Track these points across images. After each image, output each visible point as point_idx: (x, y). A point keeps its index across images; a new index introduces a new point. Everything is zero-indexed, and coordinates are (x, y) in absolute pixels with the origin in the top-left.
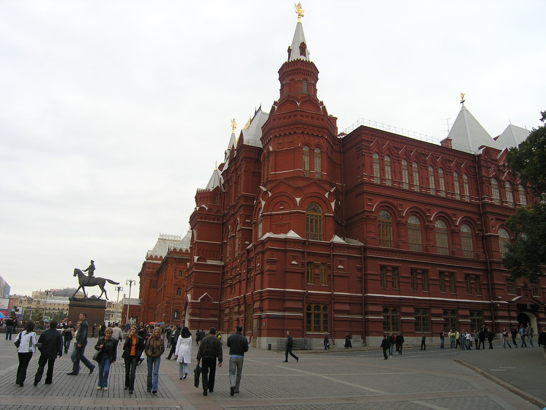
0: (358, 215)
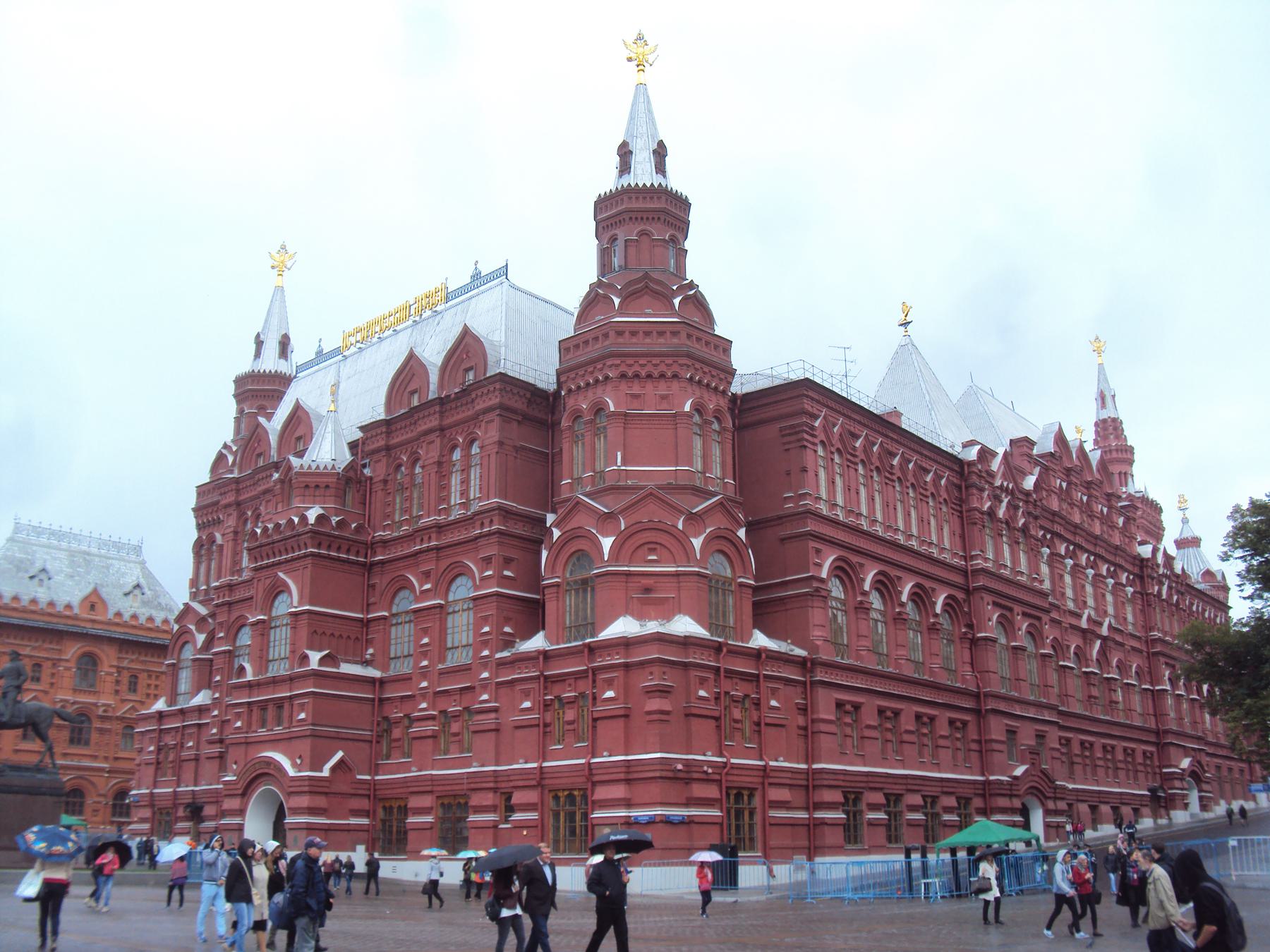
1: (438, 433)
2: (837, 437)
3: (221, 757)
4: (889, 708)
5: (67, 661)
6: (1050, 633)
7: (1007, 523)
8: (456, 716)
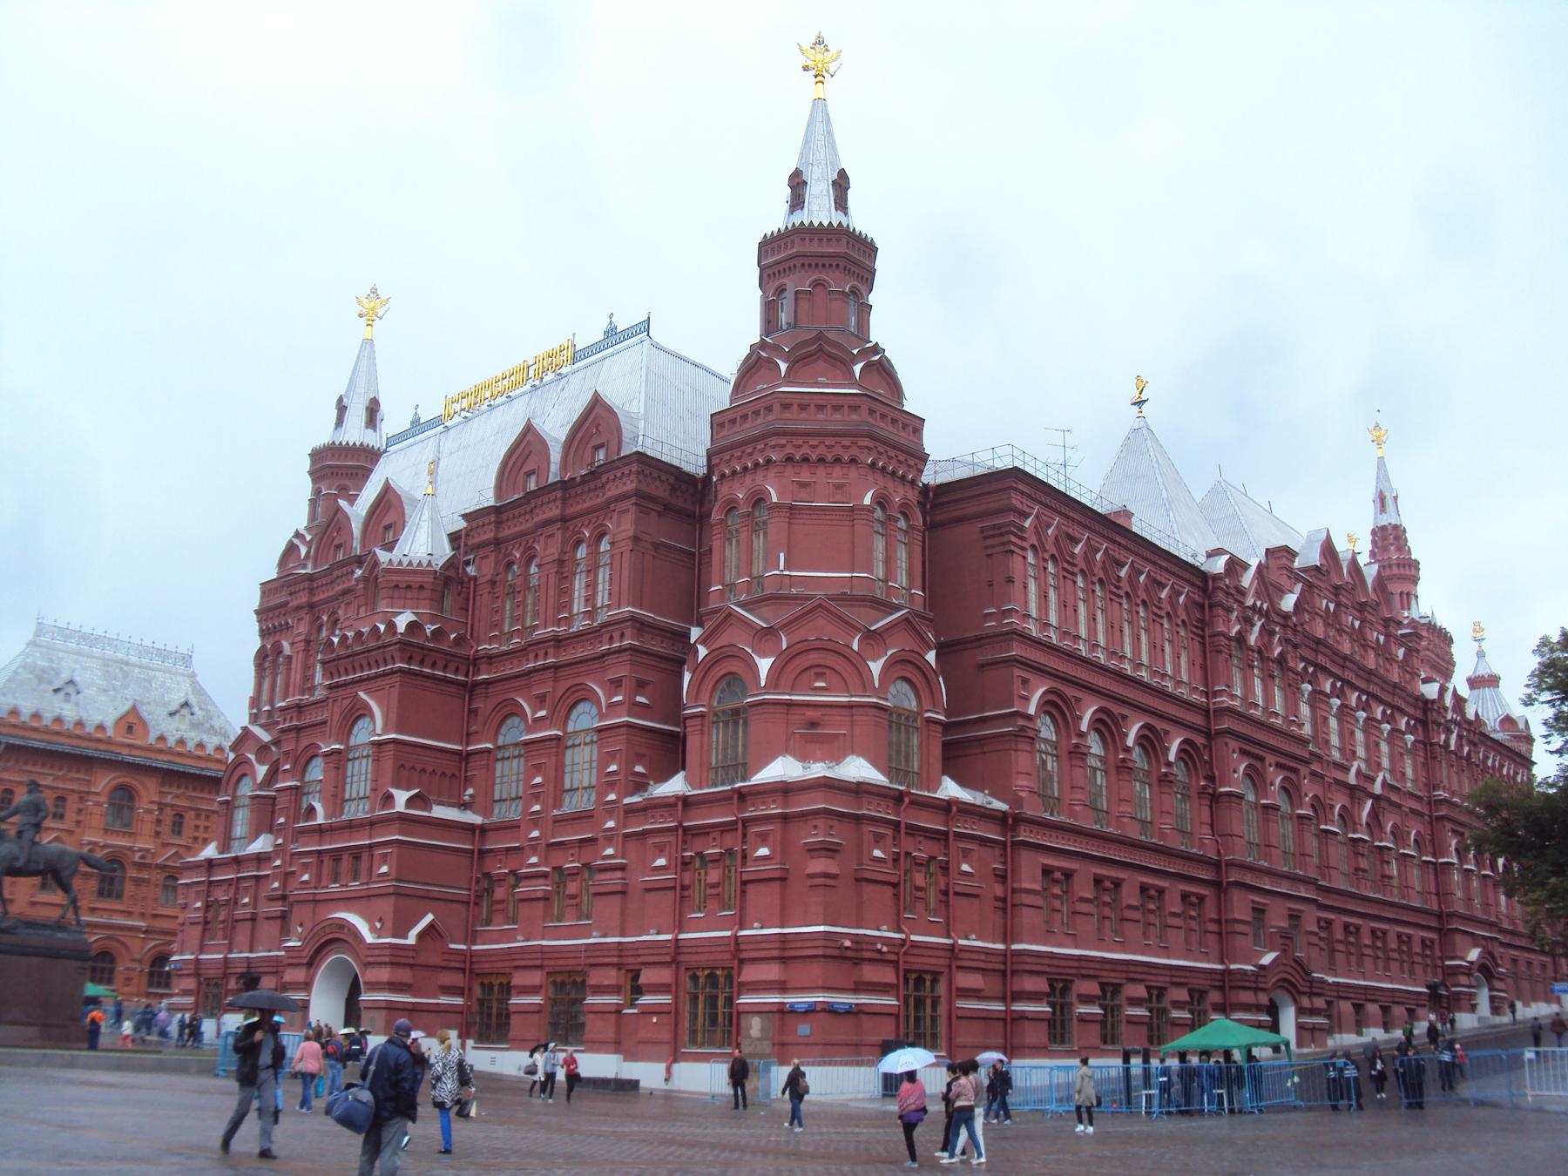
1: (558, 525)
2: (1051, 540)
3: (284, 917)
4: (1108, 878)
5: (96, 794)
6: (1310, 790)
7: (1260, 652)
8: (574, 874)
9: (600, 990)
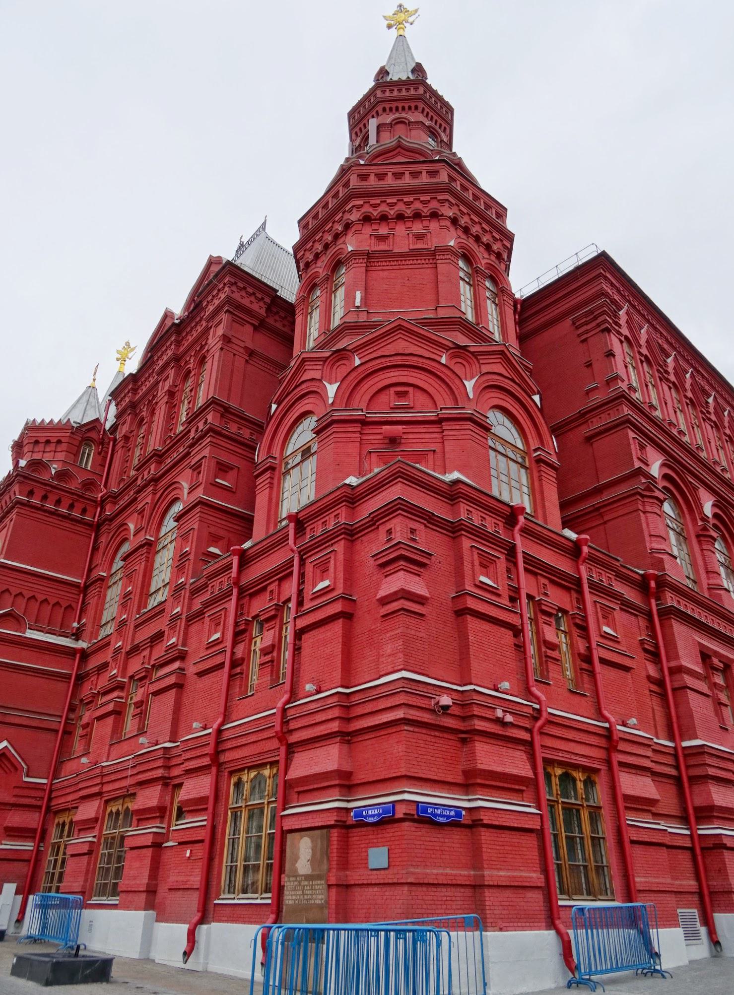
0: (599, 491)
9: (143, 816)
